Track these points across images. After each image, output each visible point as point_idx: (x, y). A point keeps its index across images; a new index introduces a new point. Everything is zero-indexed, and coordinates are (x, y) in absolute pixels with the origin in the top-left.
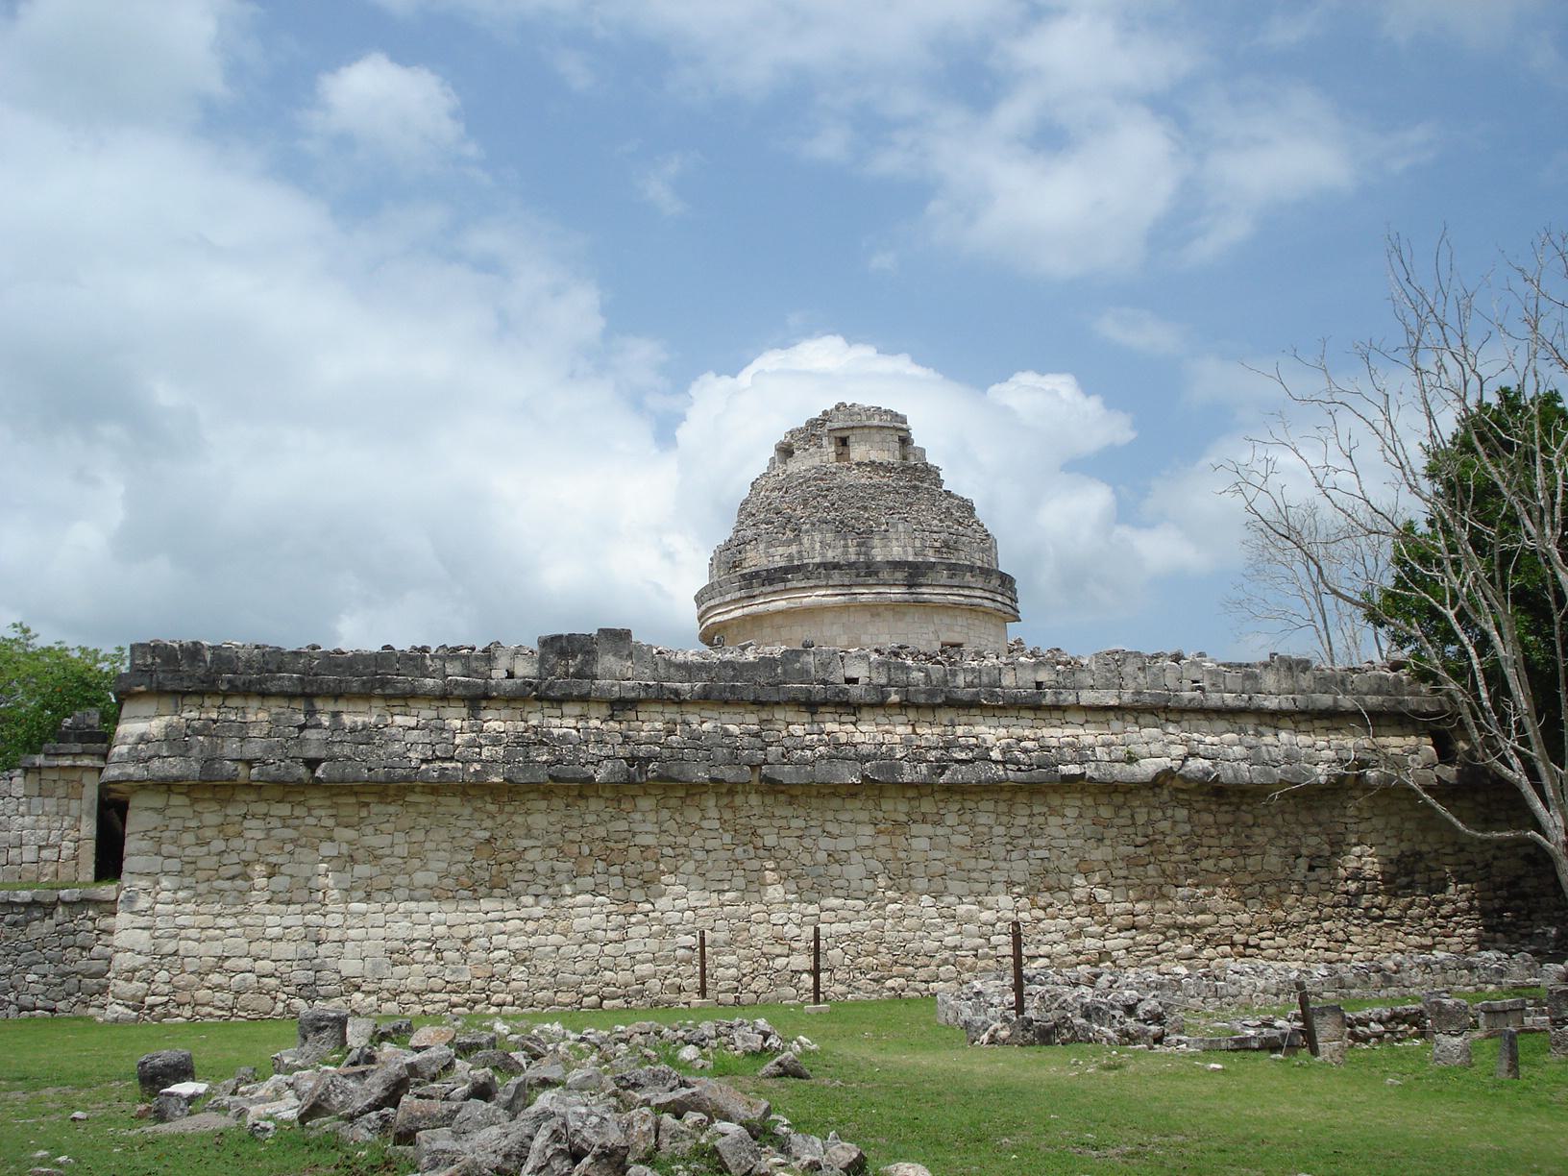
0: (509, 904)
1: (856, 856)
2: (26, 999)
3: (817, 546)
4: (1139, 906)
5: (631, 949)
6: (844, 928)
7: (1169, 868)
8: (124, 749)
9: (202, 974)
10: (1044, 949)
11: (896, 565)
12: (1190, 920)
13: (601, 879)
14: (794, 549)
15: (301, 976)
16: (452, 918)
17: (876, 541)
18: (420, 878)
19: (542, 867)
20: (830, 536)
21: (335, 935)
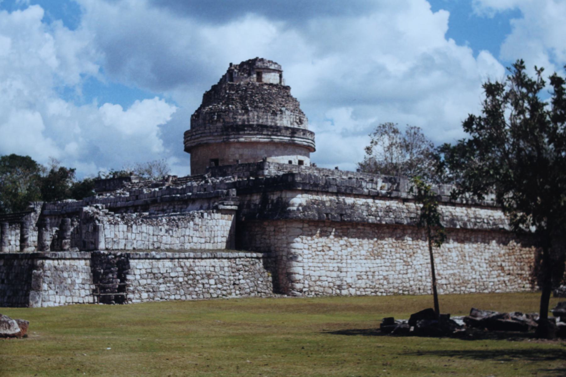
0: (382, 261)
1: (454, 250)
2: (259, 289)
3: (256, 117)
4: (511, 268)
5: (409, 275)
6: (451, 272)
7: (516, 257)
8: (295, 208)
9: (315, 281)
10: (492, 280)
11: (287, 128)
12: (520, 272)
13: (401, 254)
14: (245, 117)
15: (338, 283)
16: (371, 266)
17: (278, 117)
18: (363, 252)
19: (389, 250)
20: (261, 114)
21: (345, 270)
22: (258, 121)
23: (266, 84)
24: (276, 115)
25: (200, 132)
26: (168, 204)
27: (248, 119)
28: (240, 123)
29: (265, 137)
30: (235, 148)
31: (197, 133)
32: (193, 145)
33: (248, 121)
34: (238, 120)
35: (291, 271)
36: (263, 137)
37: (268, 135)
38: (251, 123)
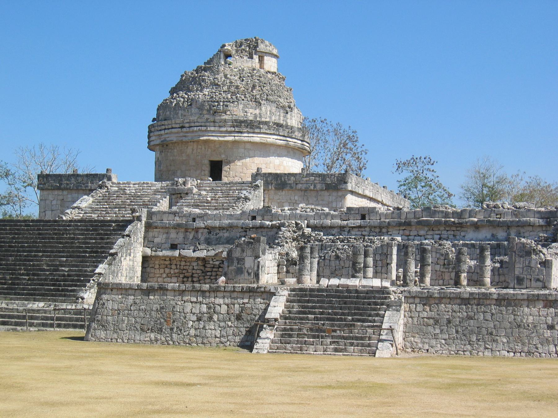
14: (257, 111)
17: (289, 116)
22: (270, 117)
23: (269, 72)
24: (287, 113)
25: (197, 124)
26: (426, 229)
27: (260, 114)
28: (251, 118)
30: (245, 149)
31: (192, 124)
32: (185, 139)
33: (261, 117)
34: (249, 114)
36: (279, 137)
37: (284, 136)
38: (263, 120)
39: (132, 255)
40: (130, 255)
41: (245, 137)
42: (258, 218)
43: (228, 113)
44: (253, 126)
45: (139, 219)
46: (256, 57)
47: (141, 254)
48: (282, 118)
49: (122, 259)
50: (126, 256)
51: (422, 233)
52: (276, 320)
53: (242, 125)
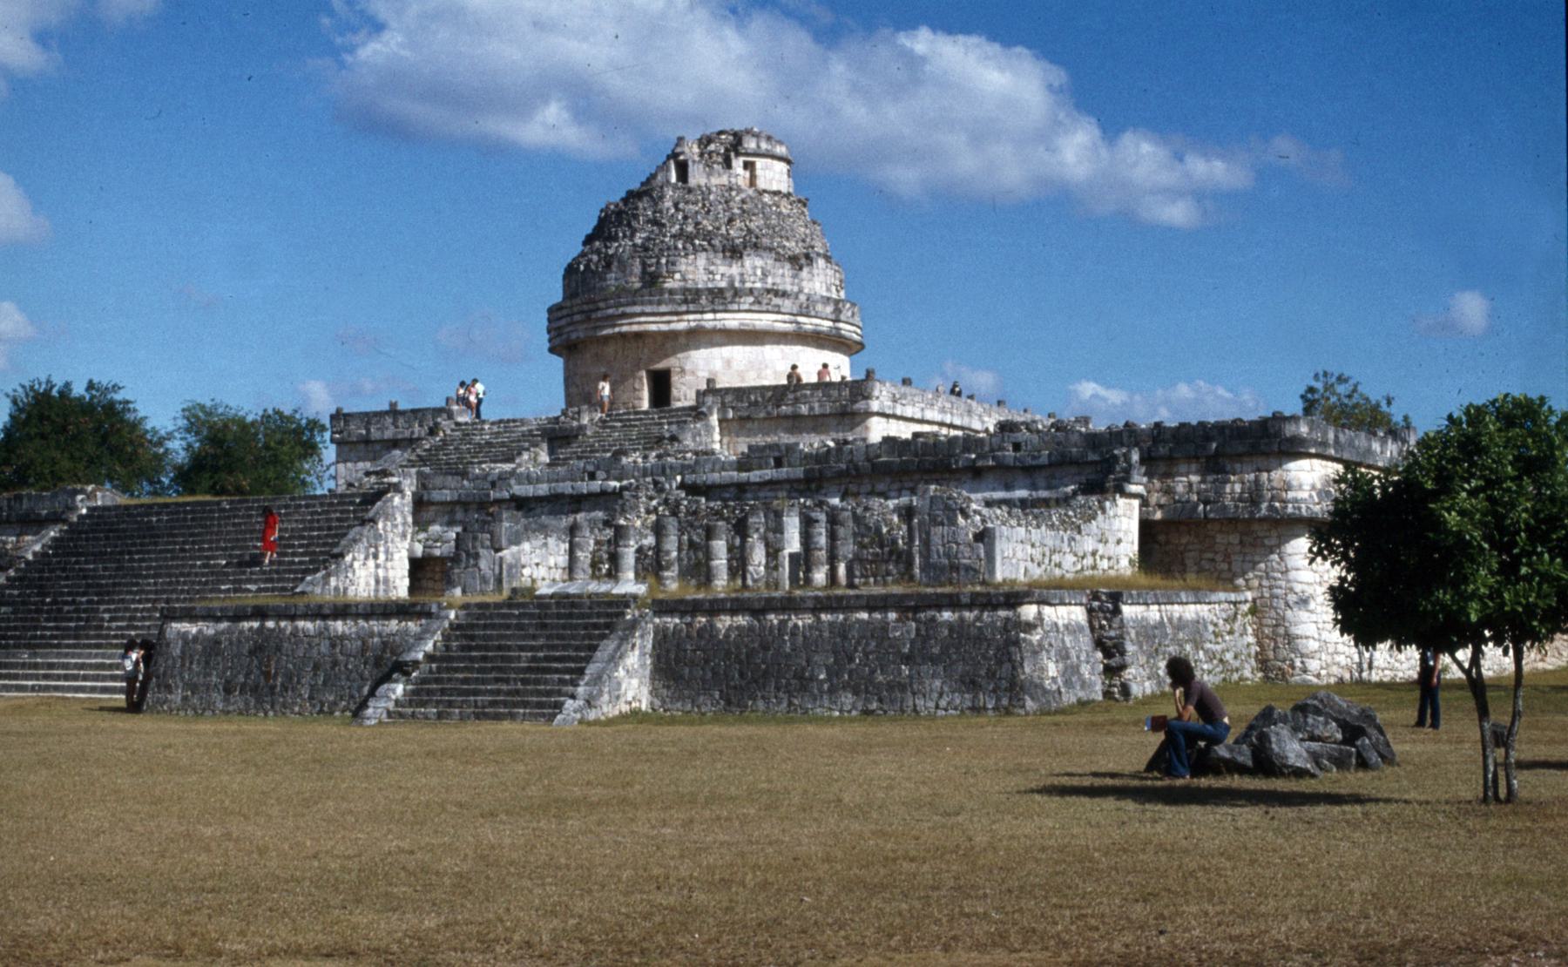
14: (735, 270)
17: (805, 273)
26: (888, 480)
27: (742, 275)
28: (723, 284)
29: (787, 317)
33: (743, 282)
35: (1299, 632)
36: (780, 317)
38: (748, 285)
39: (382, 557)
40: (376, 556)
41: (709, 320)
42: (601, 474)
43: (677, 276)
44: (720, 298)
45: (397, 488)
46: (738, 163)
47: (405, 554)
48: (788, 280)
49: (356, 564)
50: (366, 558)
51: (881, 487)
52: (416, 663)
53: (692, 297)
